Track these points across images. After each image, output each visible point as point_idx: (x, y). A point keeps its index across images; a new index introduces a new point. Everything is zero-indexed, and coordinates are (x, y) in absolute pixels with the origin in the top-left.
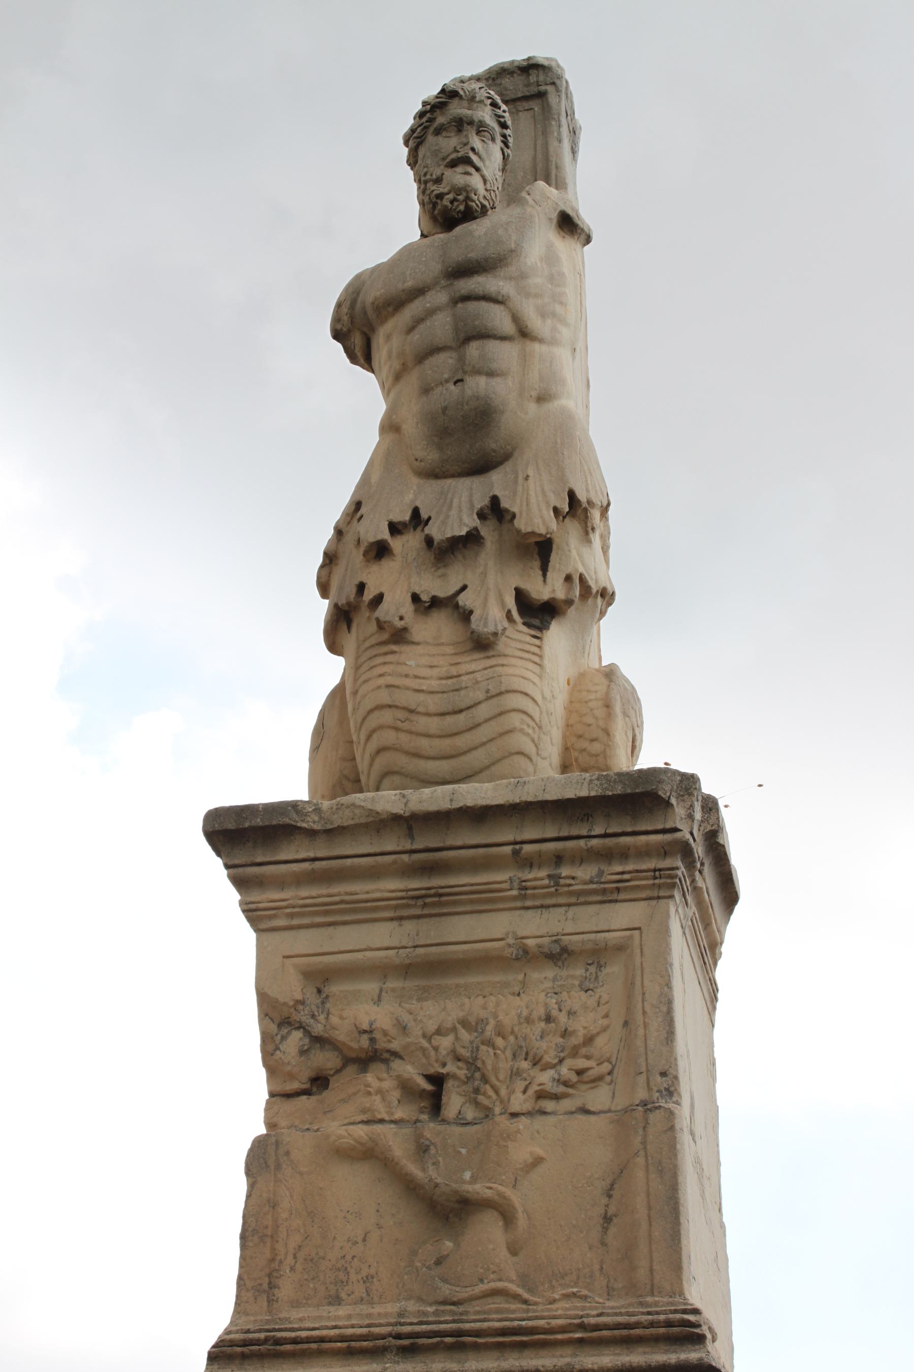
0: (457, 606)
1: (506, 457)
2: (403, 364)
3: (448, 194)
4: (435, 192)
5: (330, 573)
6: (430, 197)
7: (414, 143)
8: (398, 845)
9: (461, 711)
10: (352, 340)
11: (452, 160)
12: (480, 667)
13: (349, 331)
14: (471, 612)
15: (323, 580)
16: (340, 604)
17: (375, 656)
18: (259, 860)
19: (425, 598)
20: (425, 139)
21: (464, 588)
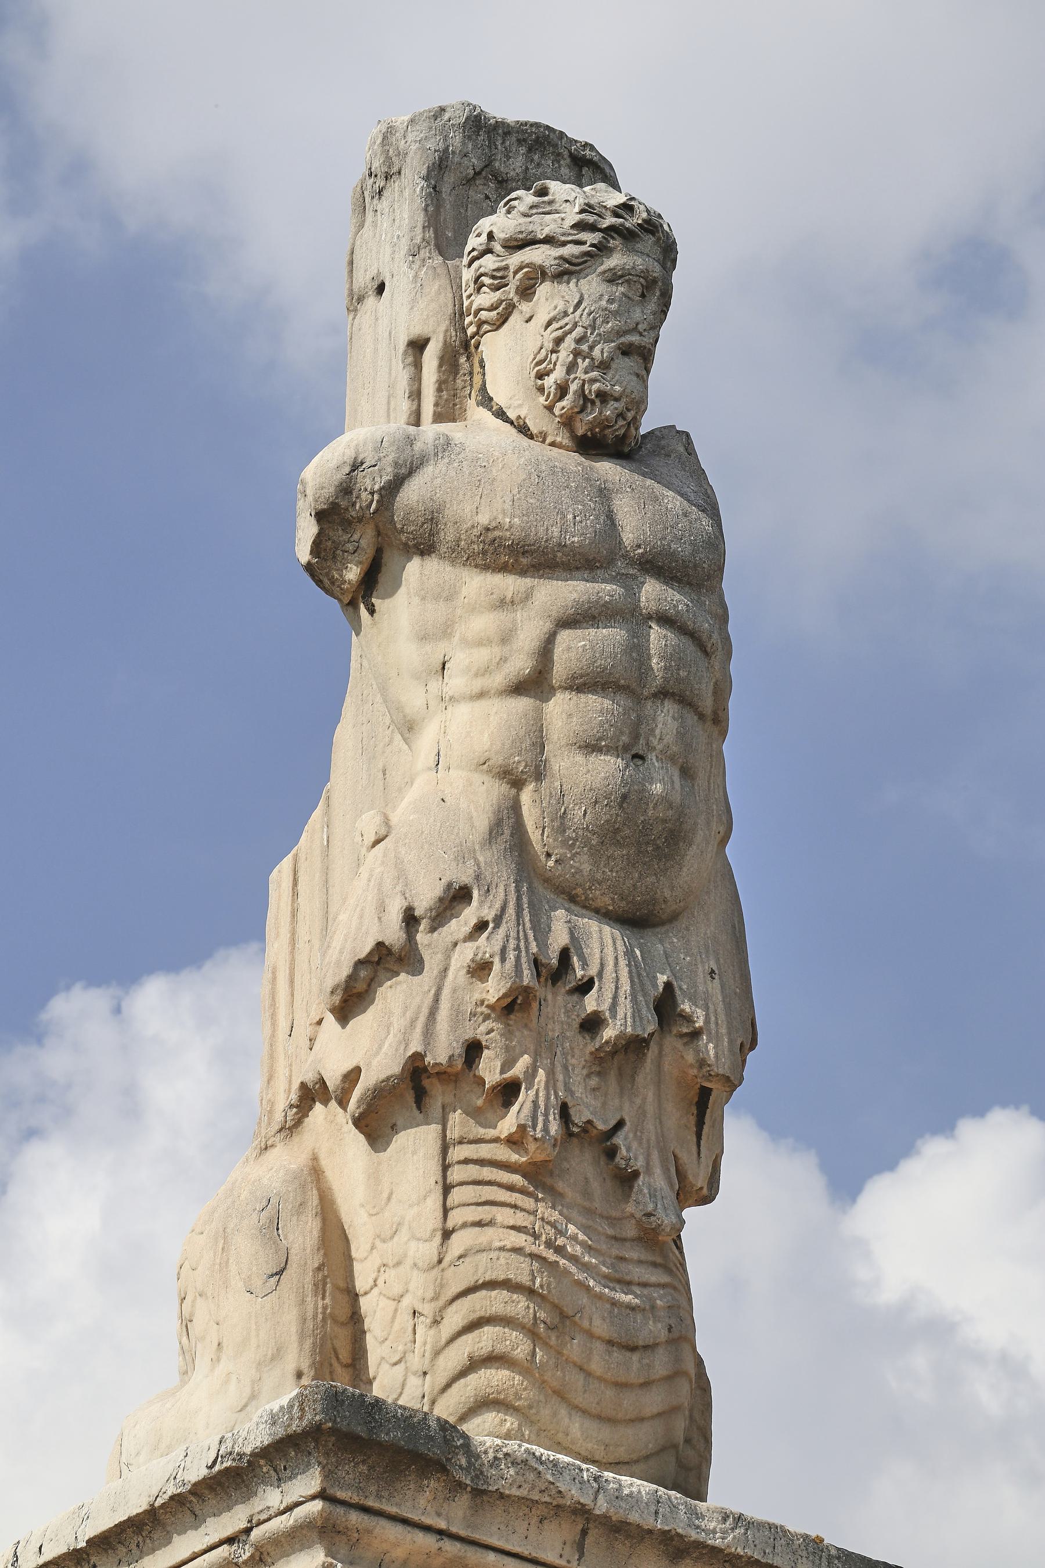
0: (611, 1153)
1: (674, 917)
2: (540, 672)
3: (617, 400)
4: (596, 386)
5: (372, 980)
6: (583, 385)
7: (559, 265)
8: (561, 1556)
9: (633, 1349)
10: (356, 537)
11: (631, 345)
12: (653, 1279)
13: (360, 520)
14: (636, 1174)
15: (361, 986)
16: (429, 1060)
17: (489, 1183)
18: (370, 1503)
19: (579, 1117)
20: (579, 272)
21: (620, 1124)
